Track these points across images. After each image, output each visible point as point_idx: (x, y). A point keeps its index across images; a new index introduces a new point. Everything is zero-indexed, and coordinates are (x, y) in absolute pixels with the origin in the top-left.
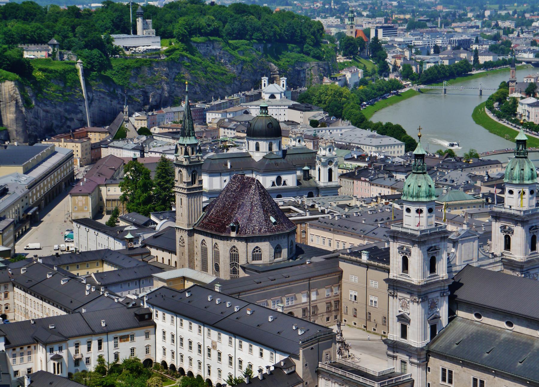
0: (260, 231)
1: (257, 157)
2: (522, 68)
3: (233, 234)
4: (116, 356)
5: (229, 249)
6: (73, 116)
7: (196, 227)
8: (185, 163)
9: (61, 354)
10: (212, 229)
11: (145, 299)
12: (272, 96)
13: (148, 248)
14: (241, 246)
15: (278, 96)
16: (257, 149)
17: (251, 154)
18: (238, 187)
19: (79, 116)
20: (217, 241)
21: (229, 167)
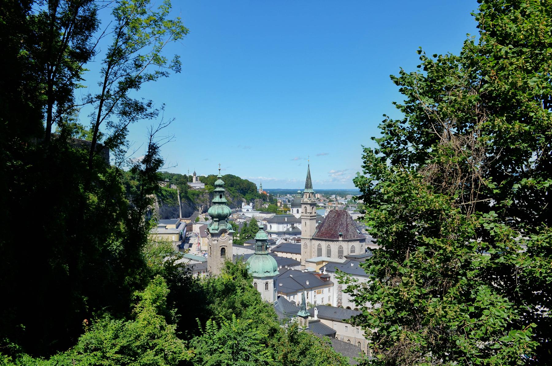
0: (354, 237)
1: (297, 216)
2: (321, 208)
3: (341, 239)
4: (315, 302)
5: (337, 247)
6: (175, 212)
7: (314, 237)
8: (309, 202)
9: (294, 300)
10: (325, 237)
11: (325, 269)
12: (248, 210)
13: (276, 253)
14: (345, 245)
15: (250, 210)
16: (298, 212)
17: (294, 215)
18: (335, 215)
19: (177, 213)
20: (330, 243)
21: (286, 220)
